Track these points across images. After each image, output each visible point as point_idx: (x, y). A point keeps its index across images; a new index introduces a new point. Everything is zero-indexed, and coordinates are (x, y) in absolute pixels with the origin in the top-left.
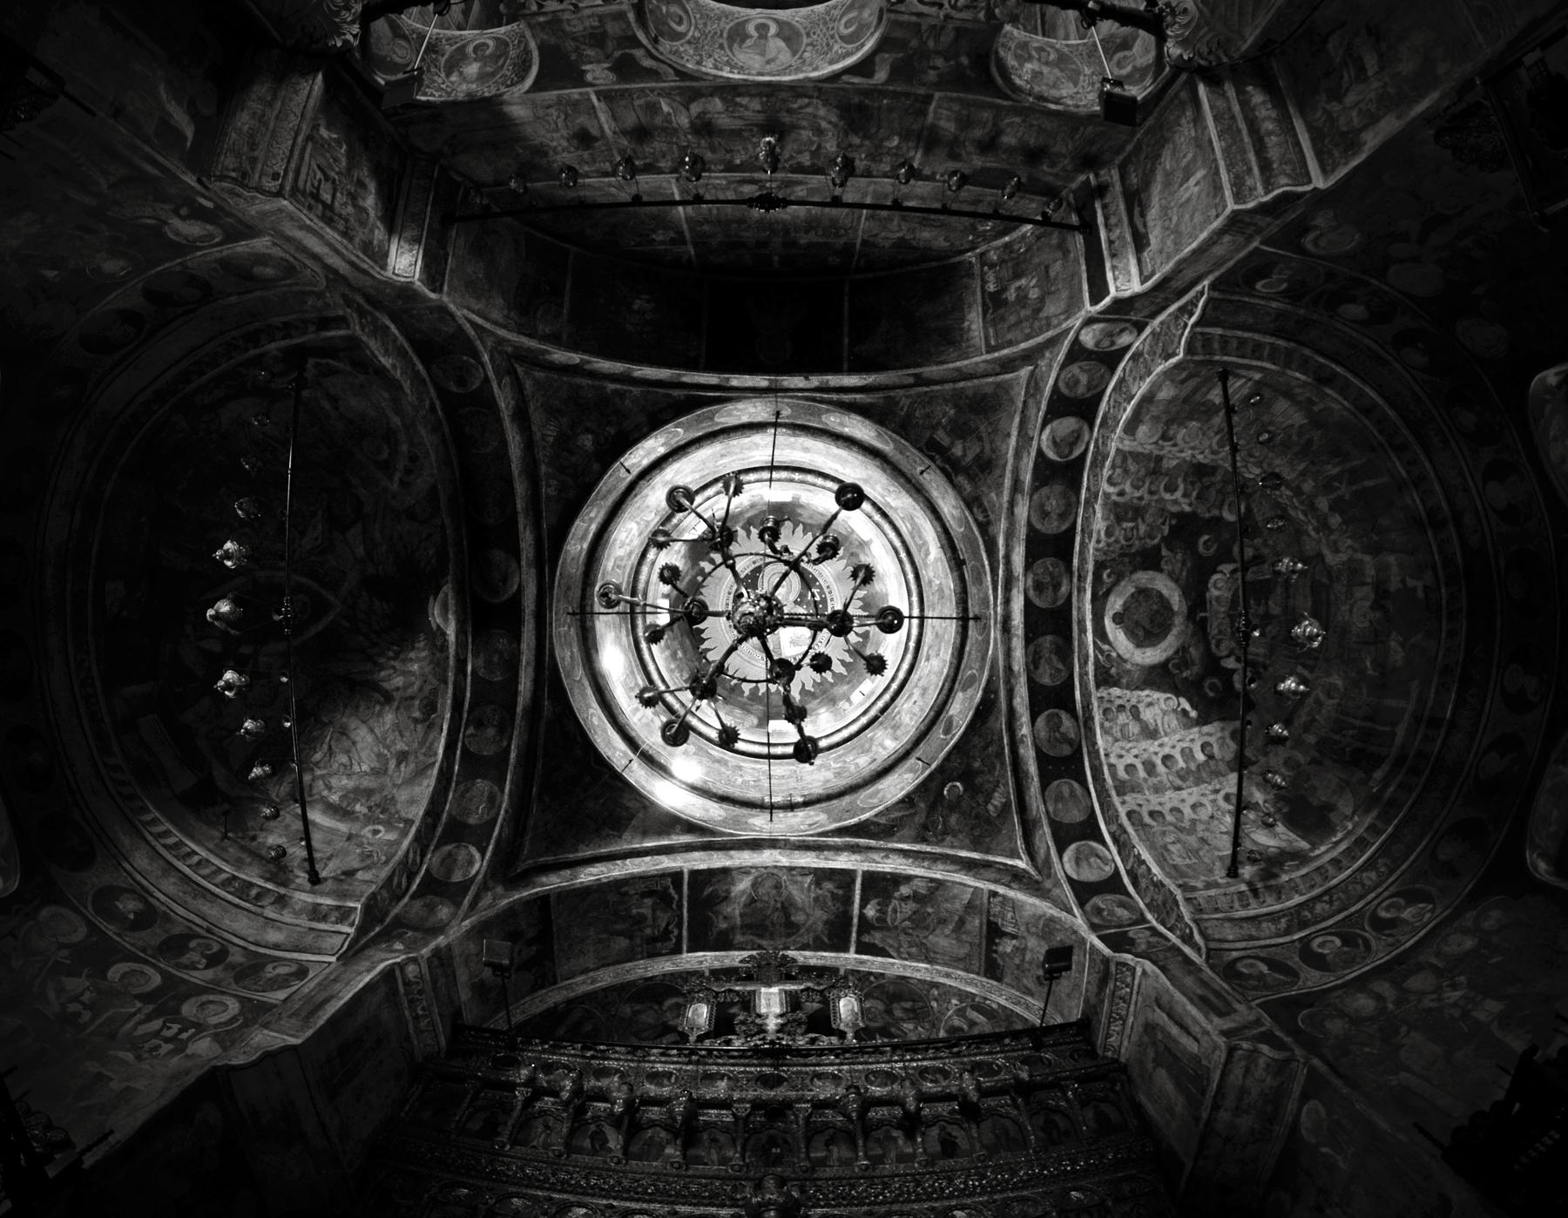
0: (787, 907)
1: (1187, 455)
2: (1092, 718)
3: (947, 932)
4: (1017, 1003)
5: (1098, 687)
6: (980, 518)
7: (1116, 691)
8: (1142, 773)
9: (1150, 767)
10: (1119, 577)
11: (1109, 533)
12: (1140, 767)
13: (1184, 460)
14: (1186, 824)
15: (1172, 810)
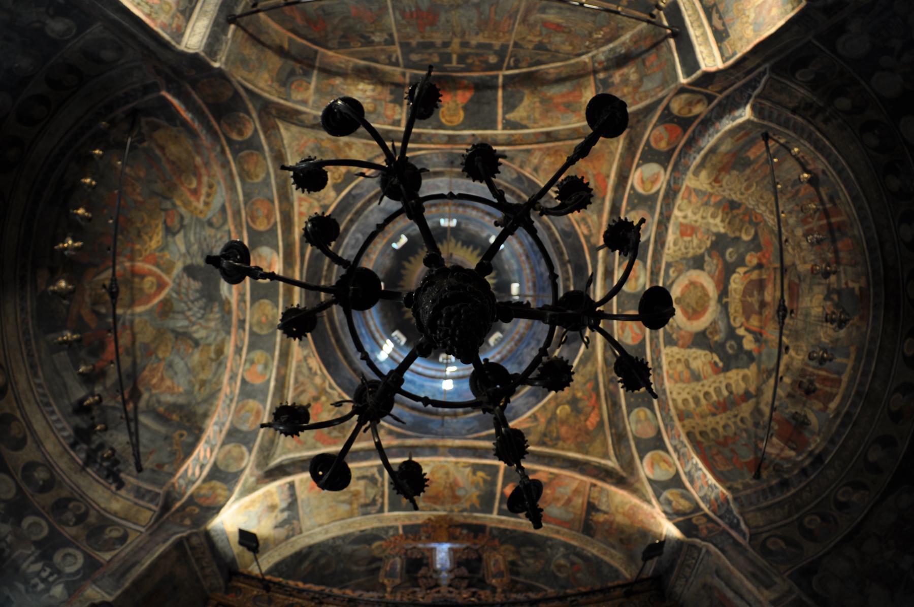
0: (453, 486)
1: (726, 194)
2: (661, 367)
3: (559, 505)
4: (605, 554)
5: (665, 346)
6: (586, 232)
7: (675, 349)
8: (692, 405)
9: (697, 400)
10: (680, 272)
11: (675, 244)
12: (691, 401)
13: (724, 197)
14: (721, 439)
15: (714, 430)
